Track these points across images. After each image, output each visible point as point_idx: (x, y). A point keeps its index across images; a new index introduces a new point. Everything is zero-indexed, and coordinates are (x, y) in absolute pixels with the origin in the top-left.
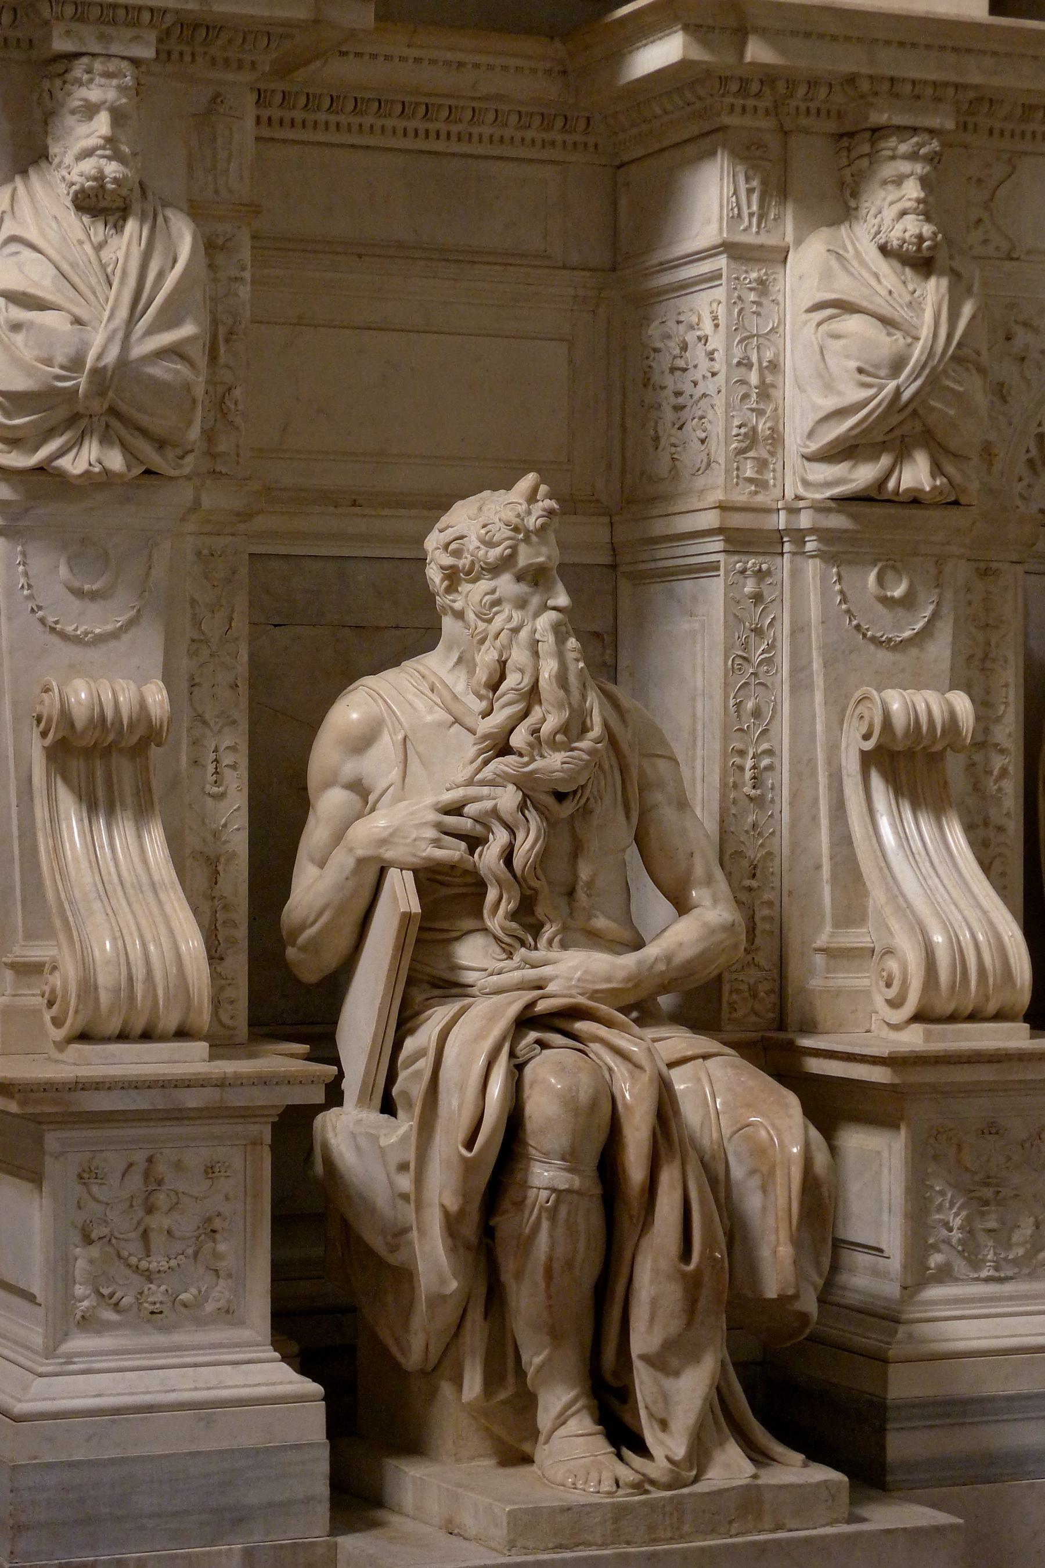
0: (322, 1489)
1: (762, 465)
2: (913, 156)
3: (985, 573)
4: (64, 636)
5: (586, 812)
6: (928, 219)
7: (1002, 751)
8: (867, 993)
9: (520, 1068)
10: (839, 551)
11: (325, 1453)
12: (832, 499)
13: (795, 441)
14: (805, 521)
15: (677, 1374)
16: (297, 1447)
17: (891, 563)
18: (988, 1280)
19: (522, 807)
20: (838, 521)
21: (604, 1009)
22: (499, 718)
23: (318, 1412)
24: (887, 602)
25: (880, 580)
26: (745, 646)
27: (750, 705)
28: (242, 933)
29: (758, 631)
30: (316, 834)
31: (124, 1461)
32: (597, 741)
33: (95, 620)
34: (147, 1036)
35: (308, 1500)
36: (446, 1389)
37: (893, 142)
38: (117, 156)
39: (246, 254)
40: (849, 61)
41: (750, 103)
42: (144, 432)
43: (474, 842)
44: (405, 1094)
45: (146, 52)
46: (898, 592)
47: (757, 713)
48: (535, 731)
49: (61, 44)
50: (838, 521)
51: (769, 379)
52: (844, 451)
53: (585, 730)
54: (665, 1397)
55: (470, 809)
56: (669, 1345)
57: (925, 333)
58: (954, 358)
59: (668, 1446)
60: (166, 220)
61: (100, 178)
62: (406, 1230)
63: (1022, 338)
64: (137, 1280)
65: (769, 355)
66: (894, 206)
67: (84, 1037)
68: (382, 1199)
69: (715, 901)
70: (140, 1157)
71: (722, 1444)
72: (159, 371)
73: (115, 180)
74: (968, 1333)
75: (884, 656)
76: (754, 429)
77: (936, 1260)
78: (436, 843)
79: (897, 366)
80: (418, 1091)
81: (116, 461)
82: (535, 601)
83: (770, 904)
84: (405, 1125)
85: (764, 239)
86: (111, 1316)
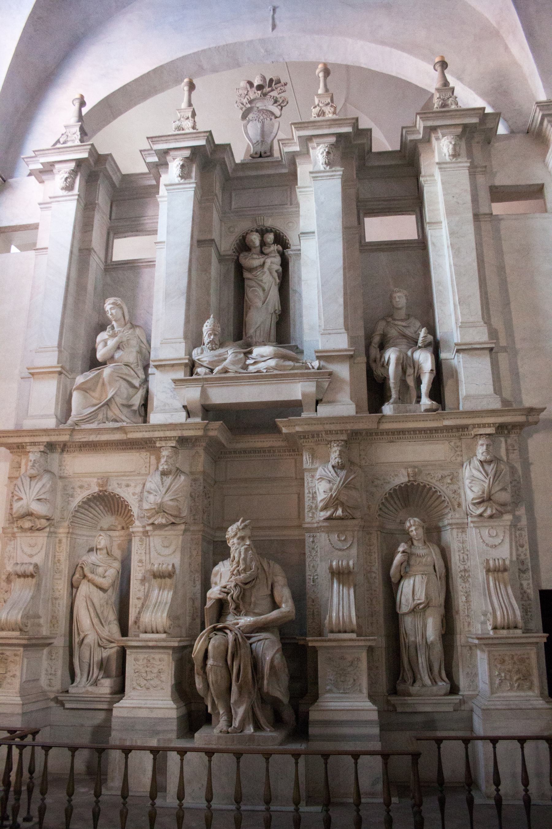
0: (175, 728)
1: (313, 513)
2: (338, 445)
3: (368, 534)
4: (160, 555)
5: (253, 587)
6: (341, 458)
7: (374, 572)
9: (210, 639)
10: (329, 531)
12: (324, 519)
14: (321, 524)
15: (239, 707)
16: (170, 718)
17: (340, 533)
18: (342, 693)
19: (236, 586)
20: (325, 524)
22: (234, 567)
24: (339, 540)
25: (338, 536)
26: (310, 552)
27: (312, 565)
29: (313, 549)
31: (134, 718)
32: (253, 571)
33: (167, 551)
35: (172, 730)
37: (332, 444)
38: (167, 464)
39: (202, 481)
40: (319, 428)
41: (307, 440)
42: (171, 515)
43: (228, 593)
45: (174, 445)
46: (343, 539)
47: (313, 567)
48: (238, 570)
49: (158, 445)
50: (325, 524)
51: (315, 495)
52: (325, 508)
53: (251, 569)
54: (236, 713)
55: (227, 587)
56: (236, 702)
57: (337, 483)
58: (345, 487)
59: (236, 723)
60: (180, 476)
61: (163, 468)
63: (377, 482)
65: (314, 491)
66: (334, 457)
67: (146, 632)
69: (287, 606)
71: (249, 724)
72: (171, 503)
73: (167, 469)
74: (333, 705)
75: (340, 553)
76: (312, 507)
77: (328, 687)
78: (220, 594)
79: (331, 490)
81: (164, 521)
82: (242, 544)
83: (318, 608)
85: (313, 467)
86: (139, 688)
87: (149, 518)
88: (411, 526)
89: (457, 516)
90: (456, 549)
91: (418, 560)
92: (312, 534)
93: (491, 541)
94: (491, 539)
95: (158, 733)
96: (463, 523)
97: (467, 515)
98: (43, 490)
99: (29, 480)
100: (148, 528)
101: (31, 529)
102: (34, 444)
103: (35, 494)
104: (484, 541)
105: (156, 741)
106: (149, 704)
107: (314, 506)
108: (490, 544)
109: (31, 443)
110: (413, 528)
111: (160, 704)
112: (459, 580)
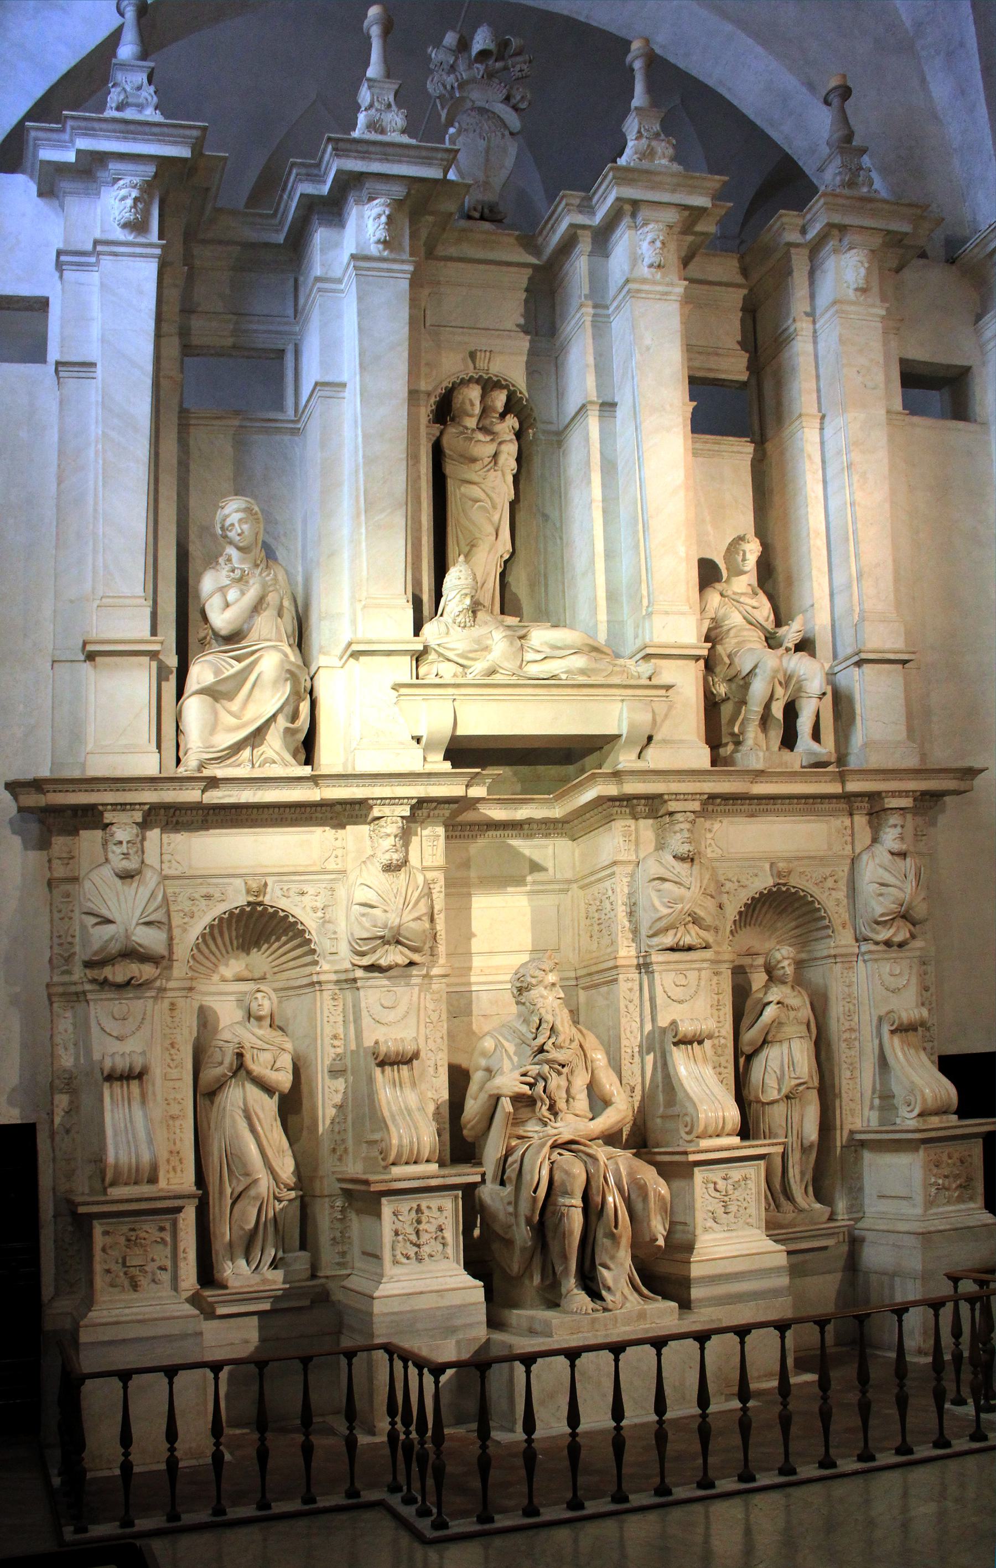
0: (484, 1318)
3: (716, 974)
8: (678, 1130)
11: (485, 1305)
13: (644, 931)
17: (681, 972)
21: (583, 1140)
23: (481, 1292)
28: (447, 1126)
30: (473, 1088)
34: (415, 1162)
36: (527, 1282)
44: (509, 1178)
62: (510, 1227)
64: (416, 1249)
68: (502, 1216)
70: (415, 1206)
80: (514, 1176)
84: (509, 1189)
85: (630, 858)
87: (362, 954)
88: (779, 962)
89: (843, 942)
90: (840, 997)
91: (792, 1014)
92: (630, 976)
93: (893, 982)
94: (892, 979)
95: (453, 1330)
96: (852, 954)
97: (857, 940)
98: (156, 904)
99: (118, 882)
100: (359, 973)
101: (128, 983)
102: (123, 807)
103: (138, 913)
104: (882, 984)
105: (454, 1342)
106: (435, 1285)
107: (632, 927)
108: (893, 986)
109: (116, 804)
110: (785, 963)
111: (451, 1283)
112: (843, 1045)
